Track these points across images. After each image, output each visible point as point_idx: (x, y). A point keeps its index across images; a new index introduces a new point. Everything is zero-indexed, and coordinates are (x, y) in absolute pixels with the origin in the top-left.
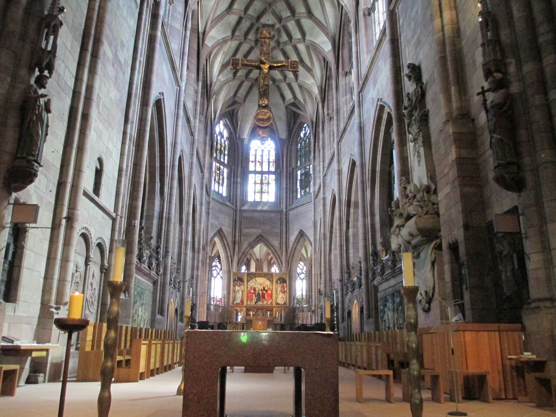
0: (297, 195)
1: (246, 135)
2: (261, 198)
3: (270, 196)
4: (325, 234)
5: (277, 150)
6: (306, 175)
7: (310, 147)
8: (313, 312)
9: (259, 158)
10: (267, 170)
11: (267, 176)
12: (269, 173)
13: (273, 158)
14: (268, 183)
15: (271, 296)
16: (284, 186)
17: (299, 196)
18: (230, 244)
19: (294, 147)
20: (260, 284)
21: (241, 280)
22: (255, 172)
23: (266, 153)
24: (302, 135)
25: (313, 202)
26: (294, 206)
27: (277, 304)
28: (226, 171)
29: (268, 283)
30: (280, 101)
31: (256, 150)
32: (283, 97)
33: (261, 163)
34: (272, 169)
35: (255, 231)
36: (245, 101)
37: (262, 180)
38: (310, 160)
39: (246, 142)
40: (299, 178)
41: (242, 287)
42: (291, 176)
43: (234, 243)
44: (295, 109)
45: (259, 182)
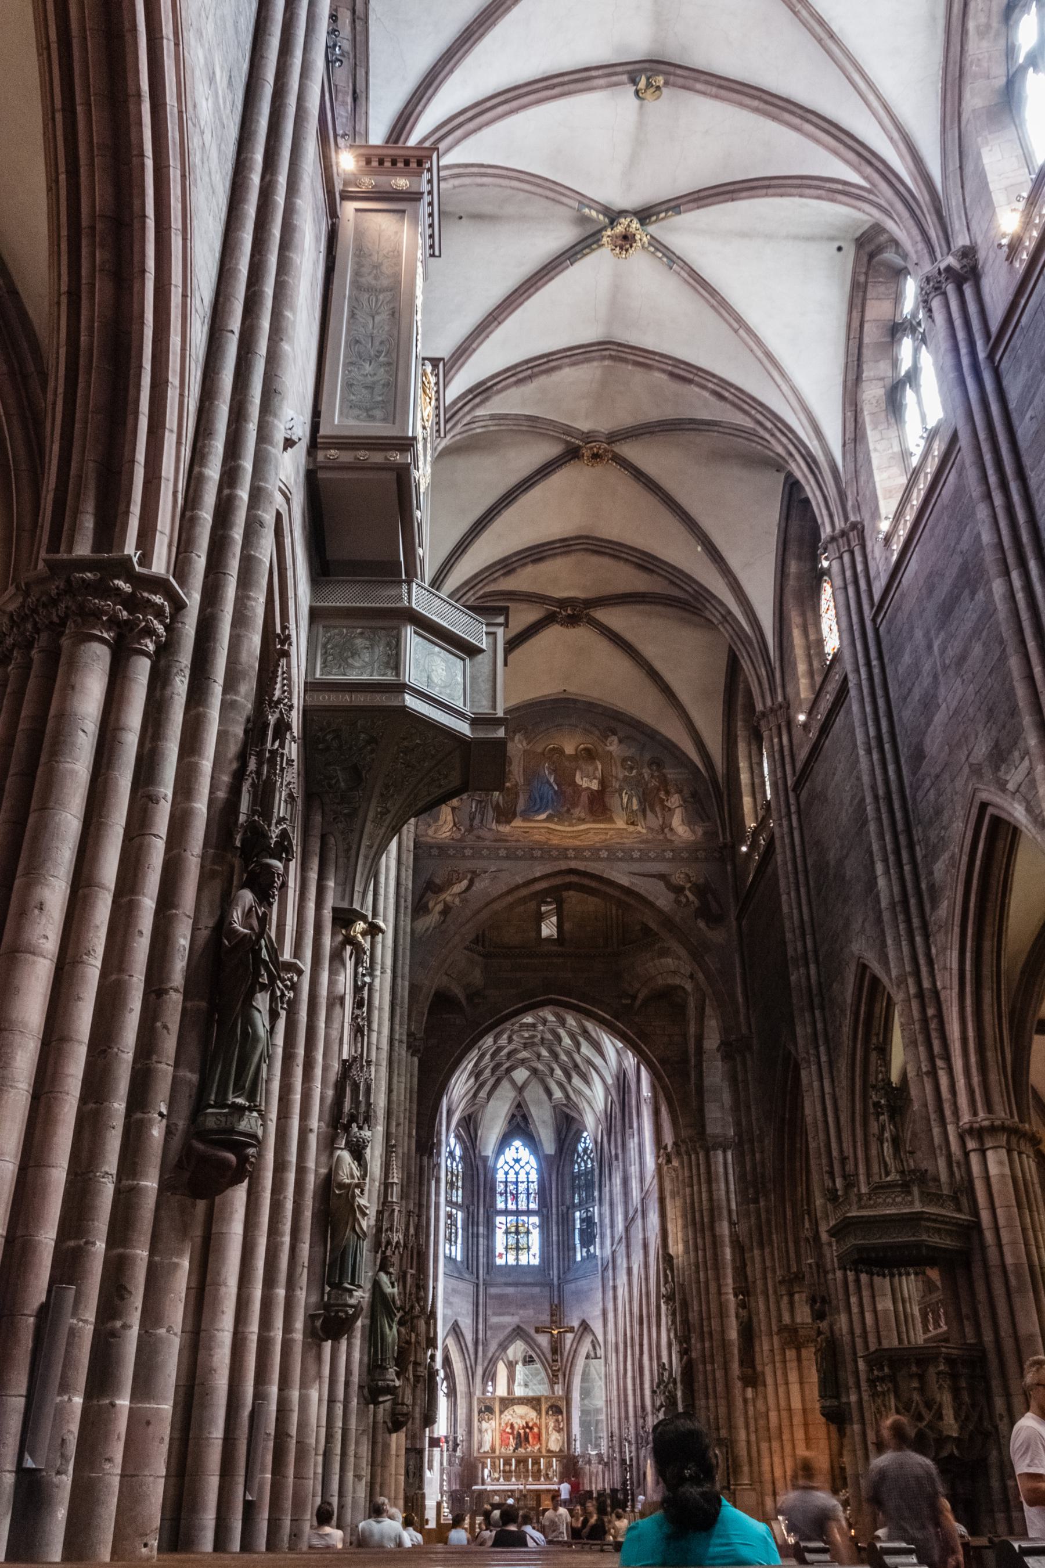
0: (575, 1255)
1: (489, 1150)
2: (517, 1259)
3: (532, 1257)
4: (617, 1344)
5: (540, 1171)
6: (588, 1221)
7: (593, 1175)
8: (606, 1464)
9: (512, 1187)
10: (524, 1208)
11: (525, 1218)
12: (528, 1213)
13: (534, 1187)
14: (528, 1232)
15: (539, 1437)
16: (555, 1238)
17: (579, 1258)
18: (470, 1345)
19: (567, 1170)
20: (521, 1417)
21: (489, 1409)
22: (506, 1212)
23: (522, 1177)
24: (580, 1149)
25: (600, 1275)
26: (569, 1277)
27: (549, 1451)
28: (460, 1214)
29: (533, 1414)
30: (545, 1097)
31: (507, 1173)
32: (549, 1093)
33: (515, 1197)
34: (533, 1206)
35: (510, 1320)
36: (488, 1099)
37: (517, 1227)
38: (594, 1200)
39: (490, 1163)
40: (578, 1226)
41: (493, 1422)
42: (566, 1221)
43: (476, 1343)
44: (568, 1111)
45: (513, 1229)
